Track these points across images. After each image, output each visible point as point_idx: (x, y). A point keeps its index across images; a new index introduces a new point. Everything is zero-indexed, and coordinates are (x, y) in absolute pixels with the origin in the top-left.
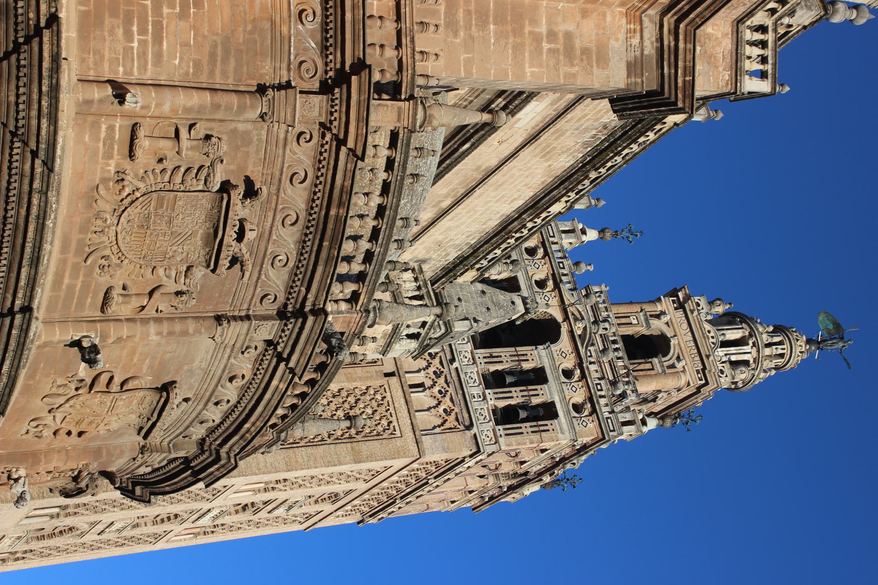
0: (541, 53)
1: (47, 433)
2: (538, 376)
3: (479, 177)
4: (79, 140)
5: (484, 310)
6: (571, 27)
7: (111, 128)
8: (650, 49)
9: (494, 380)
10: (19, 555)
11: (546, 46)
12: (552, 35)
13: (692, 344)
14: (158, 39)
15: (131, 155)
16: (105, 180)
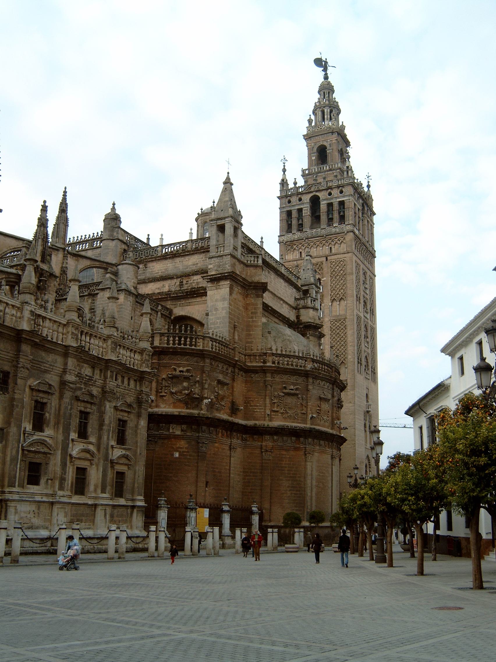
0: (255, 320)
1: (328, 419)
2: (330, 205)
3: (276, 298)
4: (275, 421)
5: (308, 270)
6: (250, 313)
7: (273, 415)
8: (254, 292)
9: (330, 220)
10: (373, 370)
11: (254, 319)
12: (252, 318)
13: (323, 136)
14: (257, 406)
15: (277, 411)
16: (282, 416)
